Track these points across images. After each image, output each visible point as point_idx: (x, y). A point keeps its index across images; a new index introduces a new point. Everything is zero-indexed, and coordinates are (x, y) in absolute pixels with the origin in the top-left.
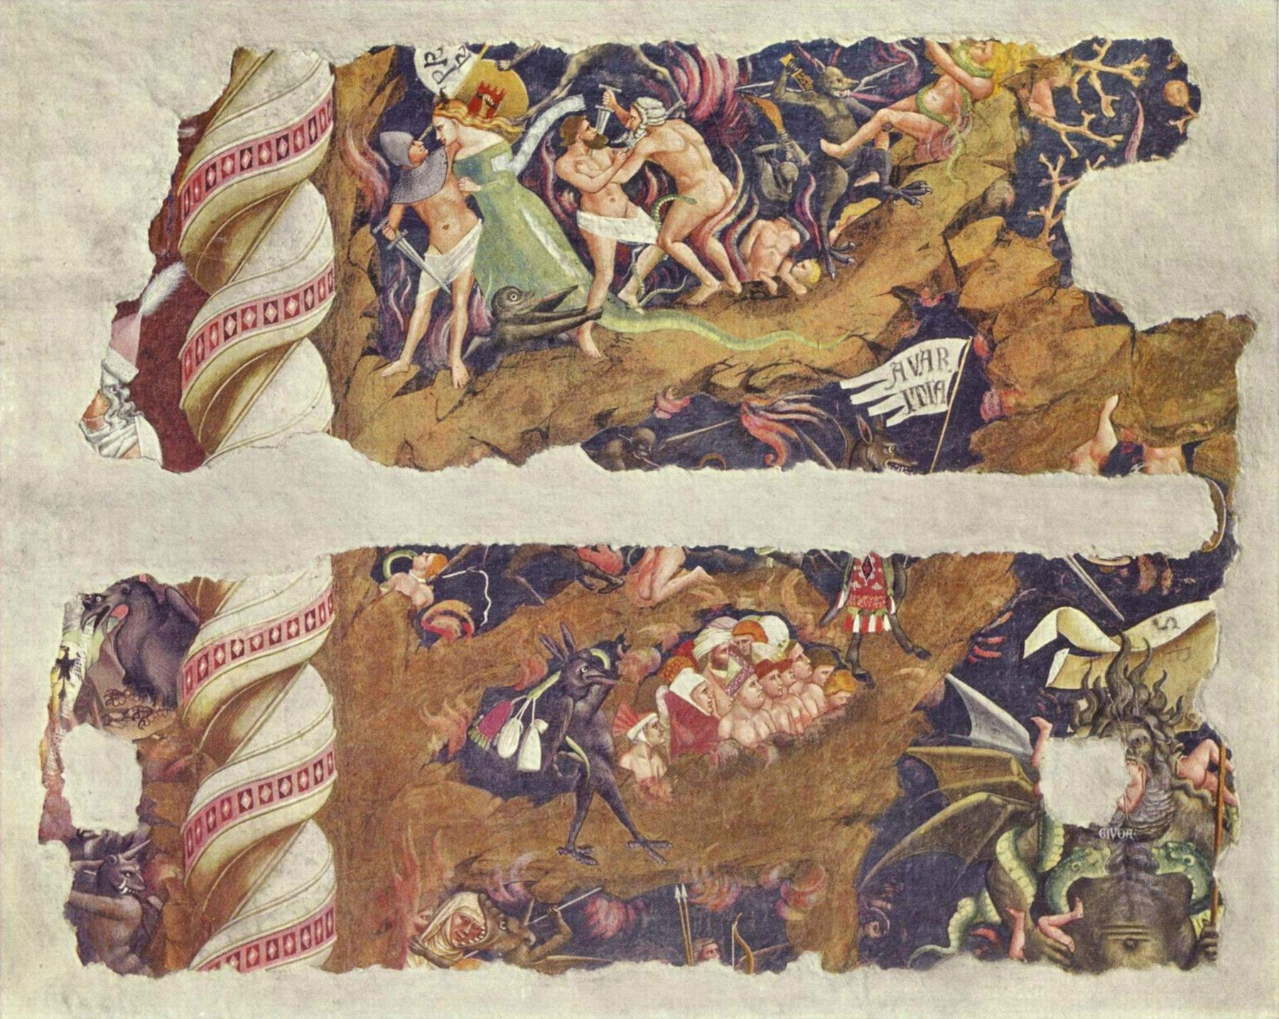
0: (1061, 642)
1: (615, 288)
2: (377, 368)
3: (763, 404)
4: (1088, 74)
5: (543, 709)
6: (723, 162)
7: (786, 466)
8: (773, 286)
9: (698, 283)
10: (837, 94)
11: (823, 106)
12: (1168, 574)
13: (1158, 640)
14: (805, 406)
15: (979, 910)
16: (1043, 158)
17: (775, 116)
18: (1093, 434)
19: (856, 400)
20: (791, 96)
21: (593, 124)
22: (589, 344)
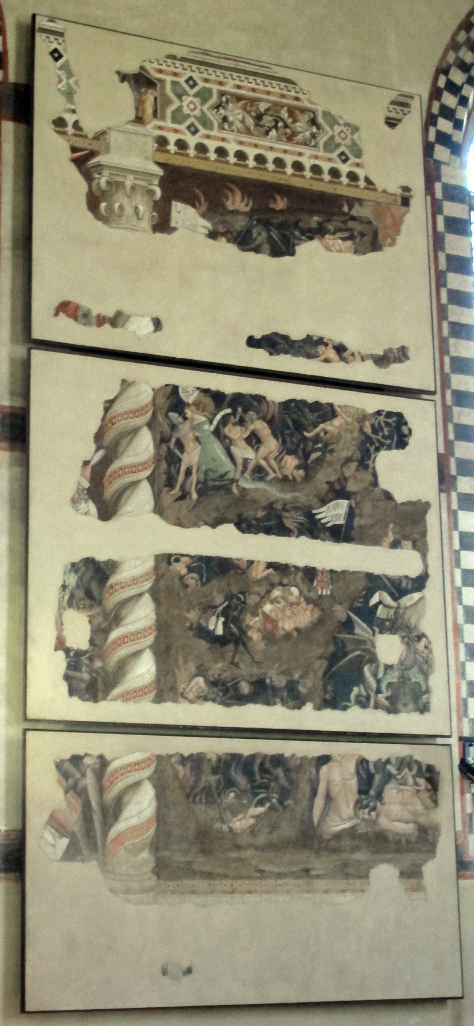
0: (380, 603)
1: (243, 472)
2: (167, 492)
3: (290, 515)
4: (380, 421)
5: (225, 613)
6: (275, 434)
7: (297, 537)
8: (291, 478)
9: (267, 474)
10: (308, 418)
11: (303, 420)
12: (410, 582)
13: (409, 604)
14: (302, 518)
15: (360, 691)
16: (368, 445)
17: (290, 422)
18: (386, 535)
19: (318, 517)
20: (294, 416)
21: (235, 417)
22: (235, 490)
